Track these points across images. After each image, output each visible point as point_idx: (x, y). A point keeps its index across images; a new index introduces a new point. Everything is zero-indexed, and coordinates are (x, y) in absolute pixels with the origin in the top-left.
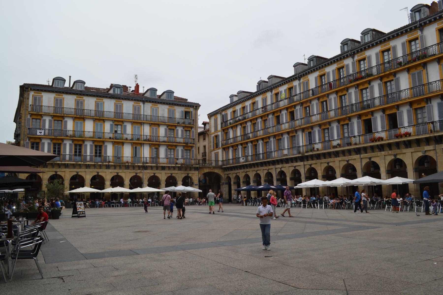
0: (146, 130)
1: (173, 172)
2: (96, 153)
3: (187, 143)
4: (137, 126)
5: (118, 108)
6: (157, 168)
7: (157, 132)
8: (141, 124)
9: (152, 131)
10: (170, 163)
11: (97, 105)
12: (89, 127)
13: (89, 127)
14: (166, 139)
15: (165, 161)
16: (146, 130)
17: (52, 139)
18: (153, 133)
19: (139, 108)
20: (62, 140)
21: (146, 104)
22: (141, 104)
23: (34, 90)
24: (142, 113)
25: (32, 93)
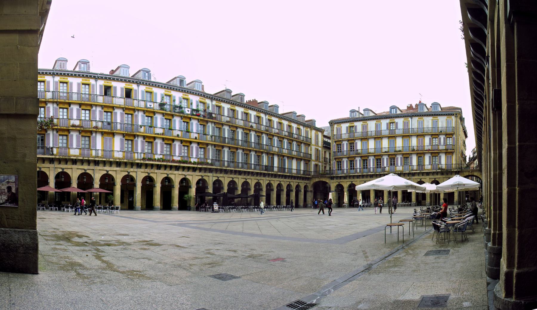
0: (414, 142)
1: (436, 176)
2: (364, 166)
3: (447, 150)
4: (406, 139)
5: (365, 127)
6: (423, 174)
7: (423, 142)
8: (410, 136)
9: (418, 142)
10: (433, 169)
11: (377, 126)
12: (371, 144)
13: (371, 144)
14: (430, 148)
15: (430, 167)
16: (414, 142)
17: (348, 158)
18: (419, 143)
19: (408, 123)
20: (355, 157)
21: (413, 118)
22: (410, 119)
23: (336, 123)
24: (410, 127)
25: (336, 126)
